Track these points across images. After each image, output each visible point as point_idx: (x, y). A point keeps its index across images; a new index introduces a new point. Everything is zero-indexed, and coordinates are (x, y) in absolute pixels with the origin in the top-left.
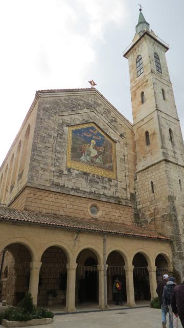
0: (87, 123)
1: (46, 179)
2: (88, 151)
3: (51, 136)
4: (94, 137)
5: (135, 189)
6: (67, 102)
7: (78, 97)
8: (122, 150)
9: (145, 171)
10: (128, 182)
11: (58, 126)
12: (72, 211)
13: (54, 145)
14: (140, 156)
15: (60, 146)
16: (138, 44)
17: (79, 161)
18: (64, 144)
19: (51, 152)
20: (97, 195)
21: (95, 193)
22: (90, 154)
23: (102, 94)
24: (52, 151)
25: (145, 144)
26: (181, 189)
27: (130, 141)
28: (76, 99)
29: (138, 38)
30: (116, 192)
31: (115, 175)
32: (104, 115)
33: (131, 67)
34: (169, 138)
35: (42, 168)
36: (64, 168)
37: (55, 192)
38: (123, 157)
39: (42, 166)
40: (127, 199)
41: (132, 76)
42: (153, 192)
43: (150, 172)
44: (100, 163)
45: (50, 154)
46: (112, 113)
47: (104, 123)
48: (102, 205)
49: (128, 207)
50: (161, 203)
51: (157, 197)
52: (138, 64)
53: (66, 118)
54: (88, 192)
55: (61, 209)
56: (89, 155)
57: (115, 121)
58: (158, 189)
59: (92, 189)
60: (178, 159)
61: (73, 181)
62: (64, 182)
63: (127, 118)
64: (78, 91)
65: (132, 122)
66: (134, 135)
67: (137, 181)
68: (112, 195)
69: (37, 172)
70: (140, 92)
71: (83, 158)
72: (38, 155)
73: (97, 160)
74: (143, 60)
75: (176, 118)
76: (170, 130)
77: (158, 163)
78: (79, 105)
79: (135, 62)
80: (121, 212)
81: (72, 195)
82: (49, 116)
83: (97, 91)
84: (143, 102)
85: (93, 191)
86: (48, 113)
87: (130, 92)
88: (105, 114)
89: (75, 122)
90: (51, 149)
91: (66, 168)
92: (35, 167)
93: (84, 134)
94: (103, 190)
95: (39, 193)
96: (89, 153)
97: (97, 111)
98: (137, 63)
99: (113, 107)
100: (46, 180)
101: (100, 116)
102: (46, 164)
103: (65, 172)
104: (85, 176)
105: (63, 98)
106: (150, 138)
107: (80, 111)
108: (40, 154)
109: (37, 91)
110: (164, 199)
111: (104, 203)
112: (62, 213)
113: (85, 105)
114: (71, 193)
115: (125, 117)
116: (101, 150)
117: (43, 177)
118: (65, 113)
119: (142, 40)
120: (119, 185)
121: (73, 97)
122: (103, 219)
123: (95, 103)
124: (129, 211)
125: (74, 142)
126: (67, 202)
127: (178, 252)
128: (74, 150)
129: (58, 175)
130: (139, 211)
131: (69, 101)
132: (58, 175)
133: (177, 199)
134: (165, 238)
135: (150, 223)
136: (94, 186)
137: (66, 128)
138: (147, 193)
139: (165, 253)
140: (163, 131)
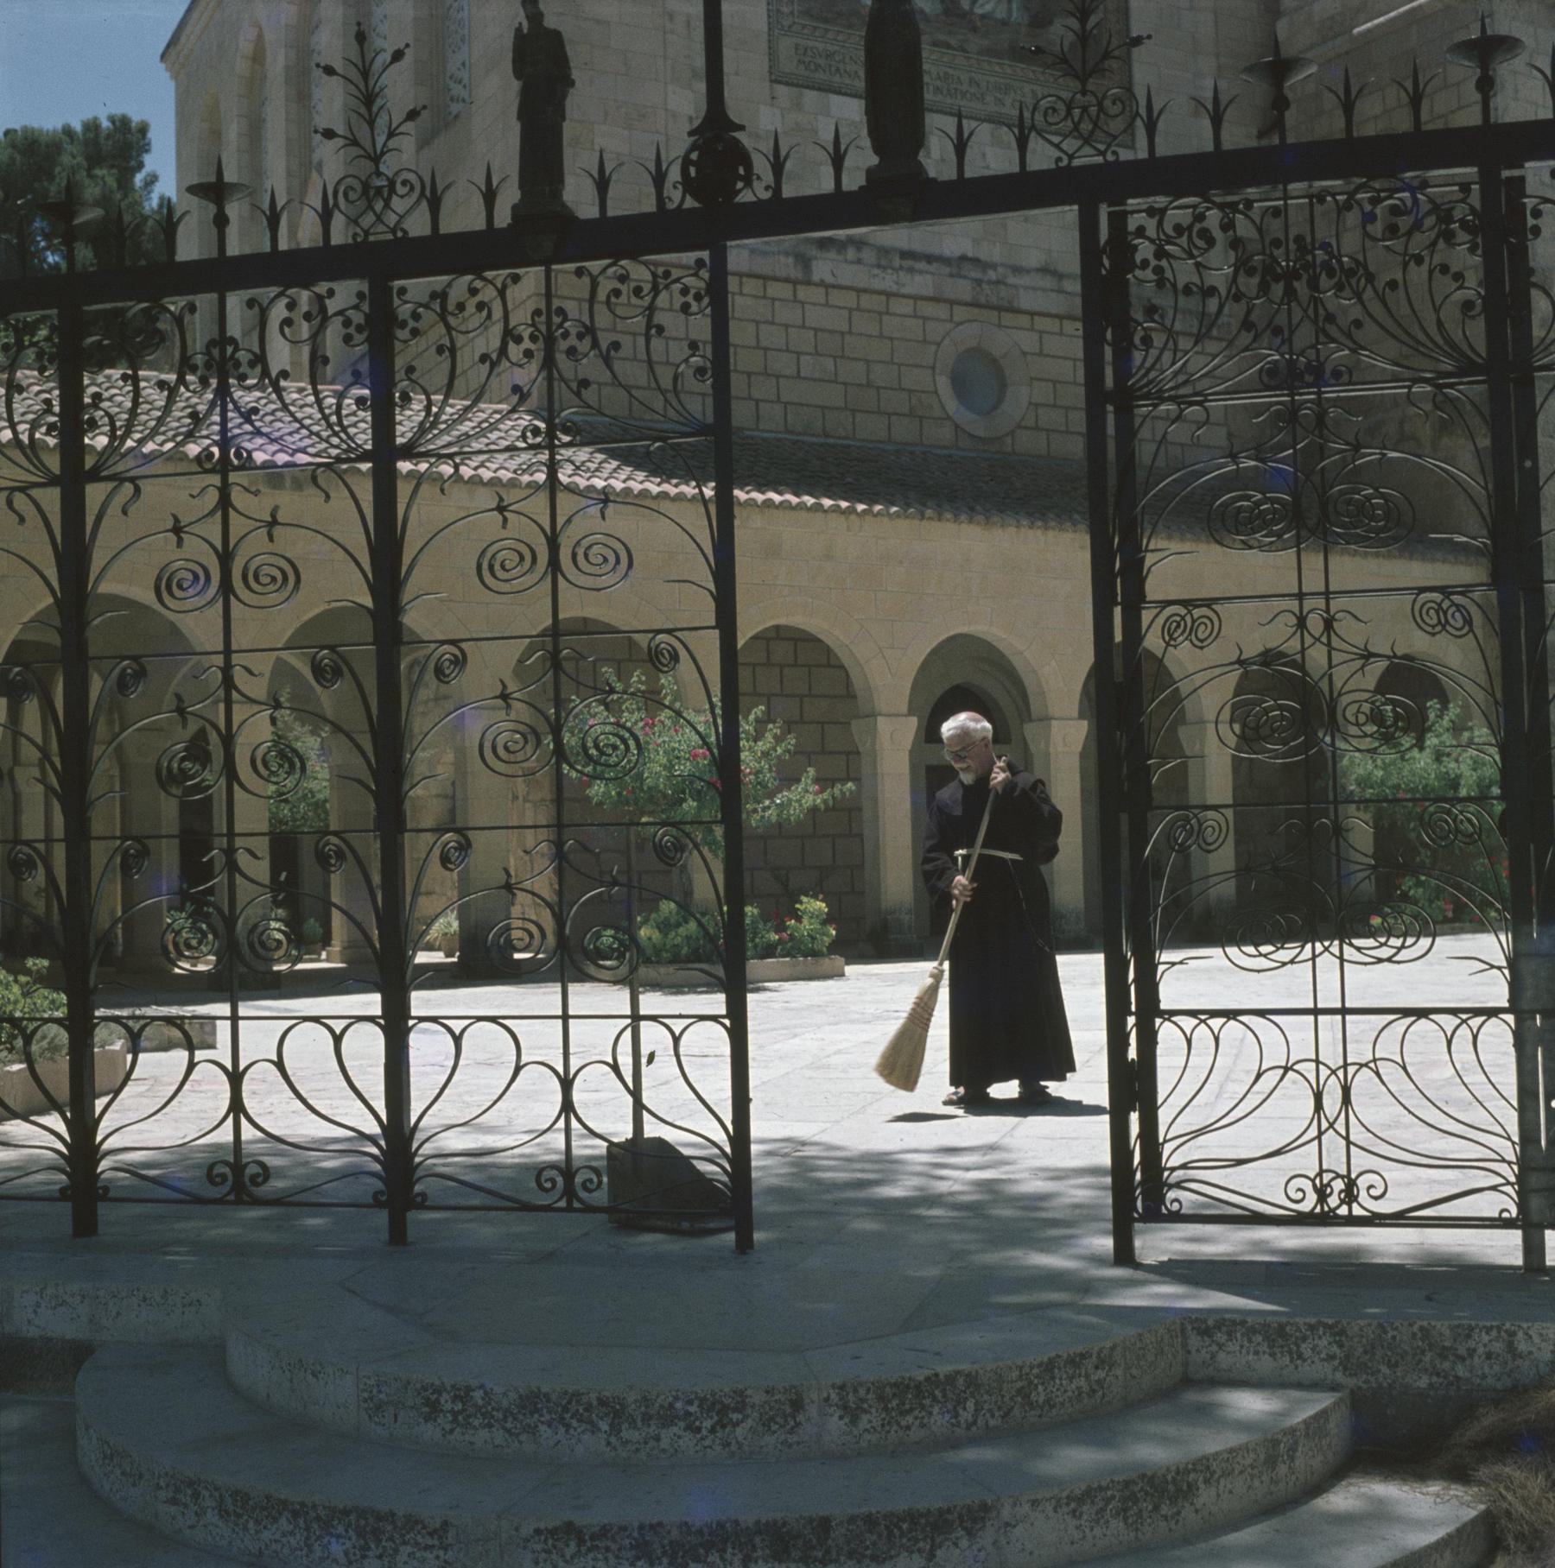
44: (1004, 23)
111: (1041, 323)
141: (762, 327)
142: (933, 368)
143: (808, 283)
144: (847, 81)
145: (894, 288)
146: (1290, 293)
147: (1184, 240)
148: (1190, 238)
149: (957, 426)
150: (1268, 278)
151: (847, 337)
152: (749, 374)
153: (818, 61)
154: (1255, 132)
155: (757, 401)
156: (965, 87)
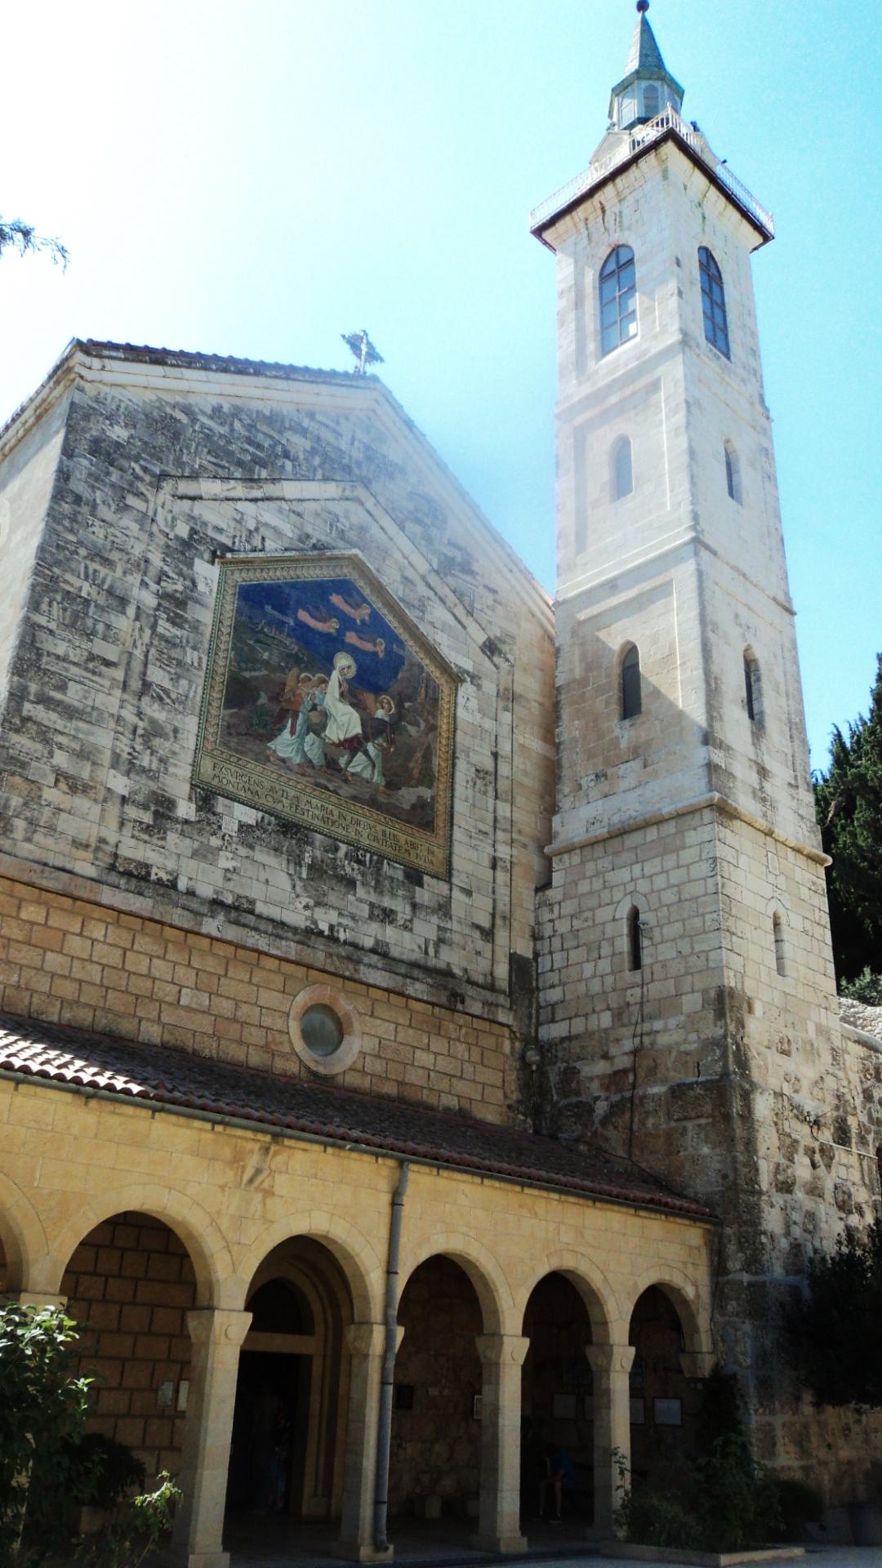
1: (83, 838)
2: (314, 707)
3: (123, 602)
4: (351, 638)
5: (536, 937)
6: (224, 430)
8: (488, 724)
9: (599, 851)
10: (503, 892)
11: (168, 552)
12: (205, 1024)
13: (139, 653)
14: (577, 766)
15: (166, 662)
17: (264, 758)
18: (191, 656)
19: (118, 693)
20: (343, 951)
21: (332, 939)
22: (324, 726)
24: (125, 687)
26: (780, 958)
27: (530, 685)
30: (441, 941)
31: (440, 854)
32: (409, 526)
35: (60, 775)
36: (178, 785)
37: (120, 912)
38: (488, 764)
39: (61, 759)
40: (491, 987)
42: (636, 963)
43: (627, 857)
44: (368, 782)
45: (110, 701)
47: (410, 573)
48: (363, 1005)
49: (496, 1029)
50: (672, 1022)
51: (655, 990)
54: (295, 930)
56: (318, 729)
57: (467, 569)
58: (667, 952)
59: (319, 913)
61: (225, 861)
62: (171, 865)
63: (530, 563)
64: (288, 378)
66: (558, 650)
67: (553, 894)
68: (417, 956)
69: (33, 798)
71: (284, 744)
72: (43, 700)
73: (358, 764)
78: (286, 455)
79: (591, 276)
80: (460, 1049)
81: (212, 938)
83: (387, 397)
84: (622, 483)
85: (324, 927)
86: (115, 476)
88: (418, 521)
89: (257, 542)
90: (119, 674)
91: (193, 786)
92: (24, 765)
93: (303, 616)
94: (374, 928)
95: (31, 912)
96: (315, 718)
97: (377, 503)
100: (76, 844)
101: (392, 528)
102: (84, 754)
103: (186, 809)
105: (207, 403)
107: (289, 489)
108: (58, 696)
110: (691, 1002)
111: (373, 992)
112: (152, 1033)
113: (317, 461)
114: (211, 926)
116: (380, 714)
117: (64, 823)
118: (207, 487)
120: (457, 910)
122: (365, 1083)
123: (369, 459)
124: (497, 1049)
125: (244, 656)
126: (185, 975)
127: (746, 1278)
128: (238, 692)
129: (147, 818)
130: (547, 1050)
131: (237, 425)
132: (147, 818)
133: (758, 1008)
134: (678, 1203)
135: (605, 1121)
136: (332, 898)
137: (207, 573)
138: (604, 966)
139: (676, 1279)
141: (155, 961)
142: (288, 1014)
143: (198, 934)
144: (250, 796)
145: (265, 948)
149: (301, 1061)
152: (137, 997)
153: (229, 778)
154: (533, 887)
156: (335, 818)
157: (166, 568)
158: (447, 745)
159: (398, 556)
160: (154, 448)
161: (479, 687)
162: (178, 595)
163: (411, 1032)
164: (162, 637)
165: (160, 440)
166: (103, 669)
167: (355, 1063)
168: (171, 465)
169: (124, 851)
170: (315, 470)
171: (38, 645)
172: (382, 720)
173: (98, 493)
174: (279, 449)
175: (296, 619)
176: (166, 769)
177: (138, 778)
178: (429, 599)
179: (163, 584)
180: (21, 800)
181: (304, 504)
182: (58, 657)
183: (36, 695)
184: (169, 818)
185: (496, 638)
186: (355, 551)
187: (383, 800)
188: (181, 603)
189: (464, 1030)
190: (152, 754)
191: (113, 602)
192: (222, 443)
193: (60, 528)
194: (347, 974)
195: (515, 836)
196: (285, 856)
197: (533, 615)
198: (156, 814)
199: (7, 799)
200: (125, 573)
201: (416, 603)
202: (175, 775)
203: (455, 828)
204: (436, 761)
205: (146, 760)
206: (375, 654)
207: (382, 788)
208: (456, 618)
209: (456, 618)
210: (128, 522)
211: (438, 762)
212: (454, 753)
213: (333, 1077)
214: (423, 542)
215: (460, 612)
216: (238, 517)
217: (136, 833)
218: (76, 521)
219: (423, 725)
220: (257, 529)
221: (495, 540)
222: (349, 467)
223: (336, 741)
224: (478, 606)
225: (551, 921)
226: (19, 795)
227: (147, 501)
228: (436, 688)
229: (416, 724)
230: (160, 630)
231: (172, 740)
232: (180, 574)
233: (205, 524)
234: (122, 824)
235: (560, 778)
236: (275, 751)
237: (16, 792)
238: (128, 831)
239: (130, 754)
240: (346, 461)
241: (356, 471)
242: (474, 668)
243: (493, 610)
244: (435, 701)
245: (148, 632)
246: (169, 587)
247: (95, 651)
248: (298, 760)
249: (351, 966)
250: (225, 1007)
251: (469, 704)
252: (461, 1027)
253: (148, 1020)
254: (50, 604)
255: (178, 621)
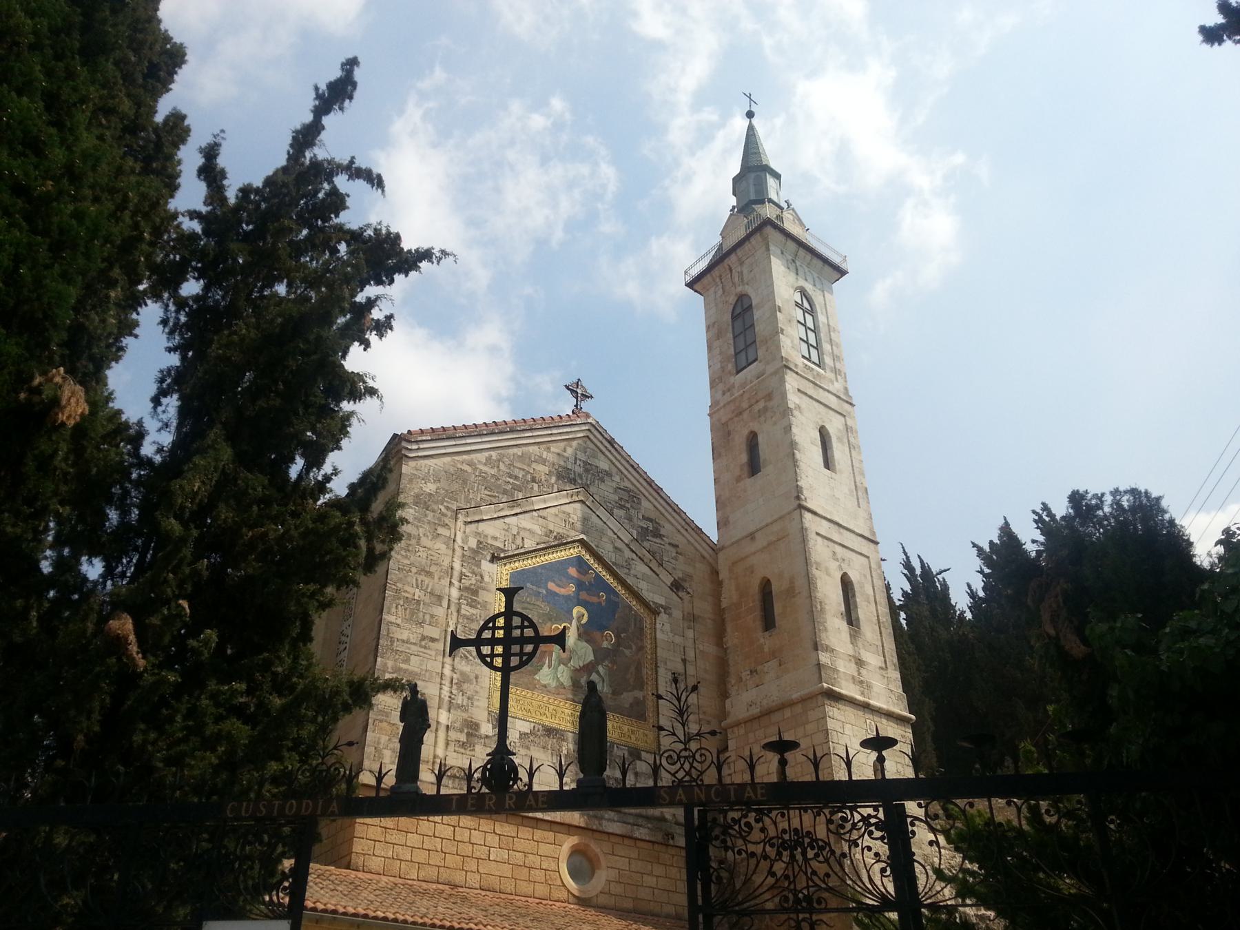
0: (561, 543)
3: (440, 598)
4: (584, 595)
6: (494, 471)
7: (531, 449)
8: (678, 639)
12: (506, 870)
16: (740, 252)
23: (613, 433)
25: (759, 624)
27: (704, 608)
28: (521, 458)
29: (741, 233)
32: (616, 511)
33: (714, 332)
34: (843, 609)
41: (719, 366)
46: (645, 503)
47: (619, 544)
52: (739, 323)
53: (488, 529)
55: (472, 865)
57: (657, 534)
60: (869, 686)
65: (713, 533)
70: (746, 432)
74: (757, 314)
75: (867, 534)
76: (847, 585)
77: (804, 700)
78: (534, 480)
79: (727, 317)
82: (434, 526)
84: (754, 466)
86: (430, 515)
87: (707, 422)
88: (622, 507)
89: (519, 541)
98: (734, 317)
99: (650, 483)
104: (551, 742)
106: (778, 608)
109: (395, 436)
111: (613, 839)
115: (691, 514)
116: (605, 644)
118: (488, 512)
119: (753, 240)
121: (515, 450)
123: (587, 471)
126: (492, 840)
129: (463, 738)
131: (502, 466)
132: (463, 738)
140: (819, 584)
141: (472, 831)
146: (792, 857)
147: (737, 827)
148: (740, 826)
149: (568, 891)
150: (780, 849)
151: (515, 839)
155: (466, 872)
157: (464, 570)
158: (652, 659)
159: (610, 533)
160: (452, 492)
161: (670, 615)
162: (472, 587)
163: (640, 863)
164: (464, 616)
165: (456, 486)
166: (431, 644)
167: (603, 888)
168: (463, 502)
169: (450, 762)
170: (553, 486)
171: (391, 635)
172: (607, 648)
173: (421, 529)
174: (529, 477)
175: (549, 591)
176: (472, 704)
177: (455, 712)
178: (632, 559)
179: (463, 581)
180: (387, 738)
181: (547, 510)
182: (403, 641)
183: (392, 668)
184: (476, 736)
185: (679, 578)
186: (582, 536)
187: (611, 704)
188: (474, 591)
189: (676, 858)
190: (463, 695)
191: (434, 599)
192: (493, 481)
193: (399, 557)
194: (594, 827)
195: (701, 716)
196: (550, 751)
197: (704, 557)
198: (468, 734)
199: (379, 738)
200: (439, 579)
201: (624, 564)
202: (478, 707)
203: (660, 716)
204: (645, 671)
205: (459, 700)
206: (600, 603)
207: (610, 696)
208: (652, 570)
209: (652, 570)
210: (440, 546)
211: (647, 671)
212: (656, 664)
213: (590, 899)
214: (626, 521)
215: (654, 565)
216: (506, 527)
217: (457, 749)
218: (408, 551)
219: (634, 647)
220: (518, 533)
221: (675, 511)
222: (575, 480)
223: (578, 668)
224: (665, 558)
225: (730, 775)
226: (386, 735)
227: (450, 529)
228: (641, 621)
229: (630, 647)
230: (463, 612)
231: (475, 683)
232: (473, 573)
233: (486, 536)
234: (447, 744)
235: (728, 672)
236: (539, 681)
237: (384, 732)
238: (451, 748)
239: (450, 697)
240: (572, 476)
241: (580, 482)
242: (666, 602)
243: (677, 560)
244: (642, 629)
245: (455, 614)
246: (466, 582)
247: (425, 634)
248: (554, 685)
249: (597, 822)
250: (518, 858)
251: (664, 628)
252: (673, 856)
253: (472, 871)
254: (397, 607)
255: (472, 605)
